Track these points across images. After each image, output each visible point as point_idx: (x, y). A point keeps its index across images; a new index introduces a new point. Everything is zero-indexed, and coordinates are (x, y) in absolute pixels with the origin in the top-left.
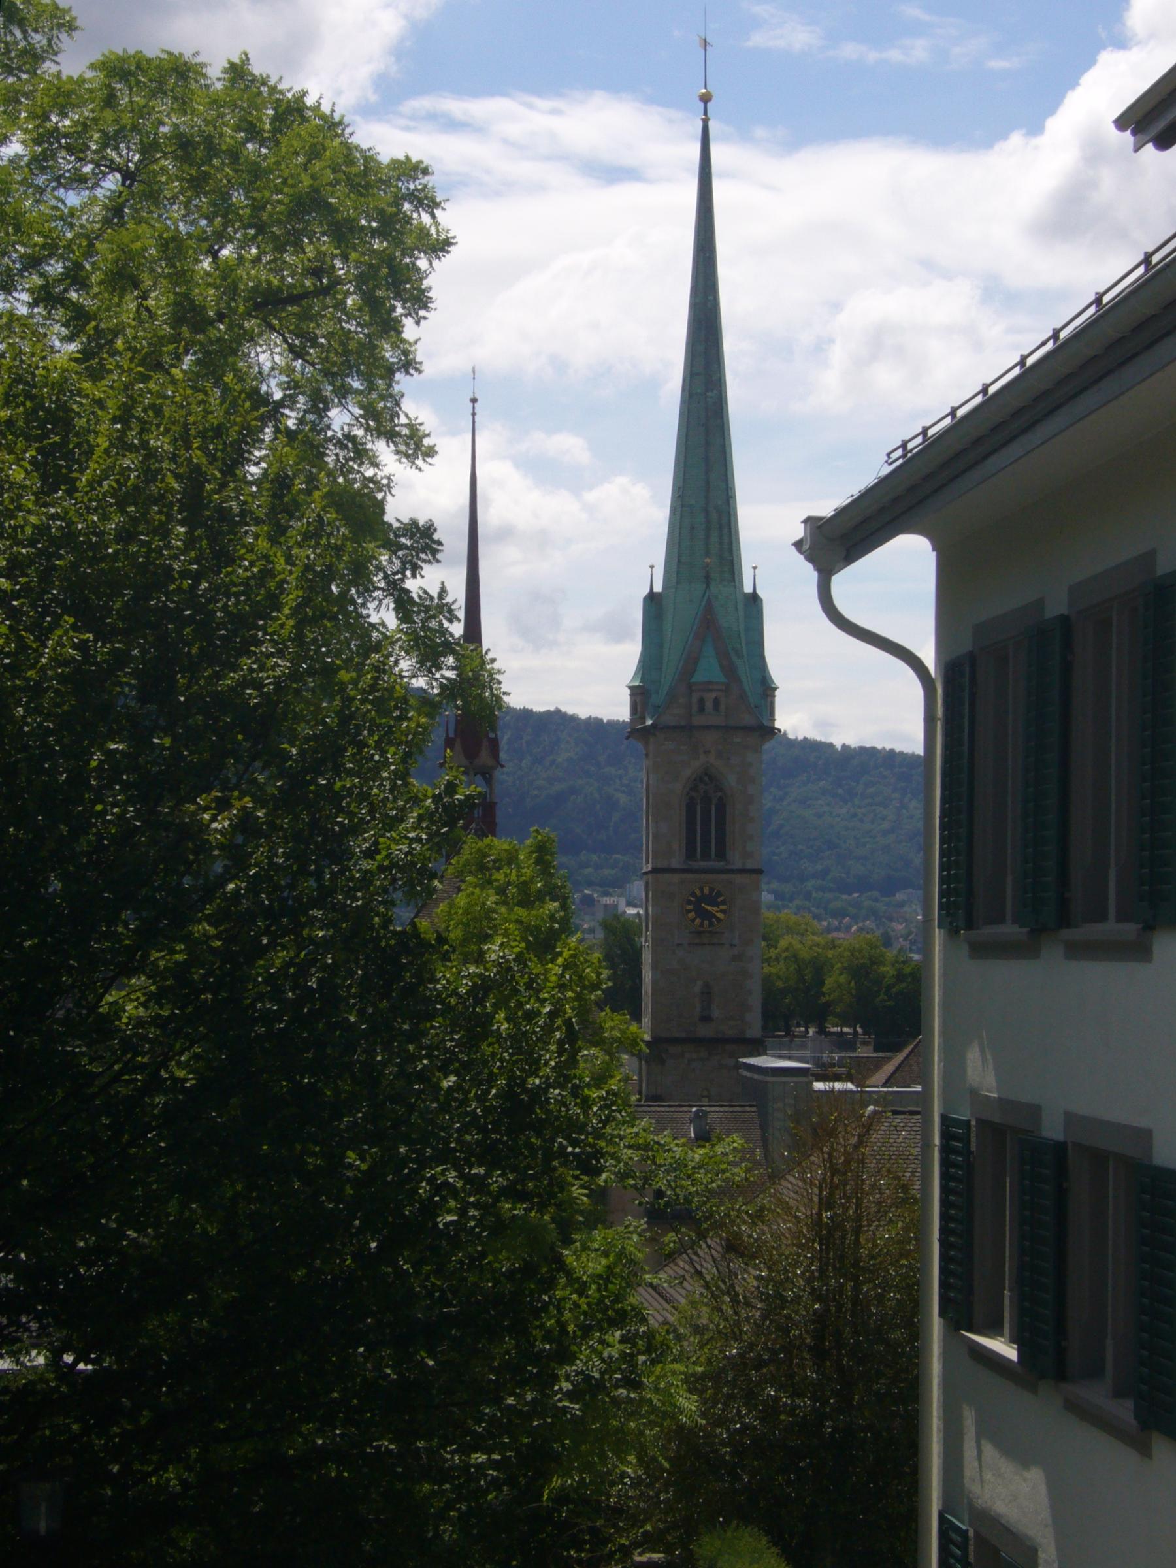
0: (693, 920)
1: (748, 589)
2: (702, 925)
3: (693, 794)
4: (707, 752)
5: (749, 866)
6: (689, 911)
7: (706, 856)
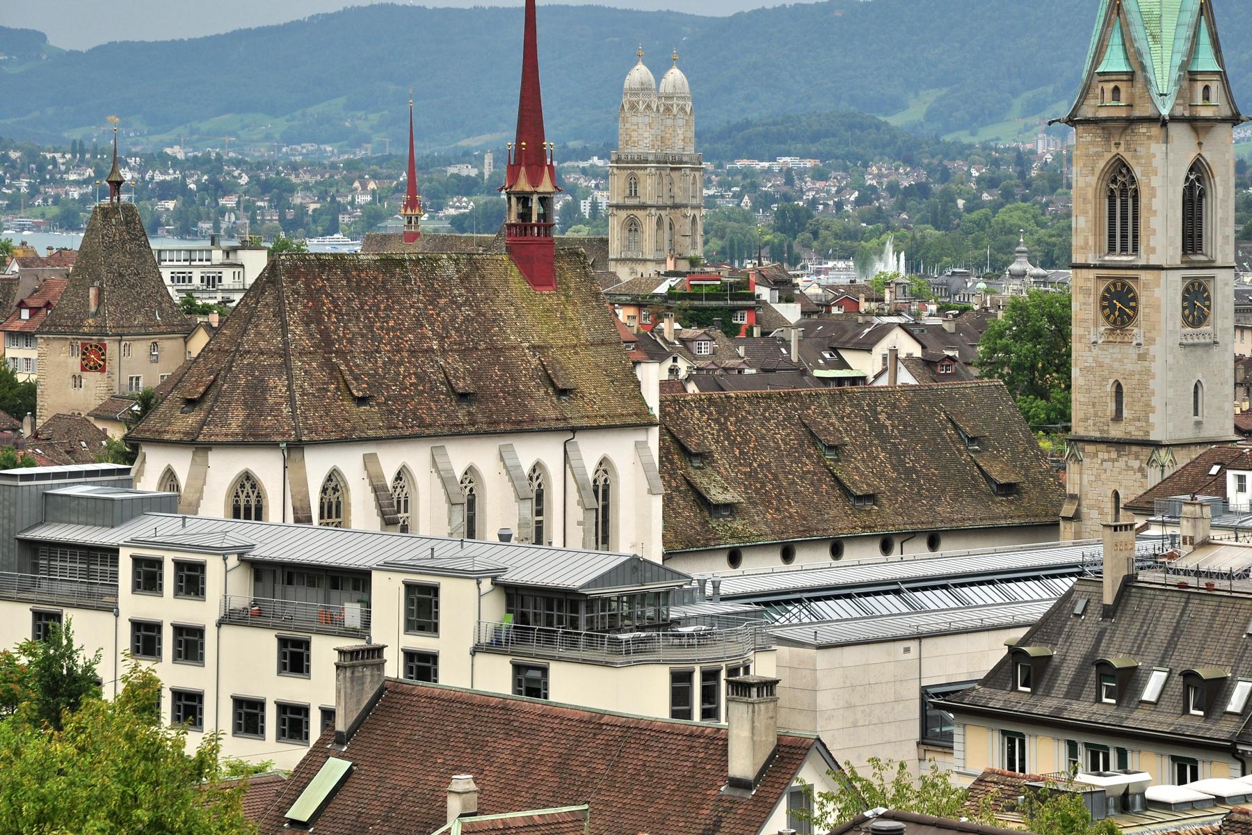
3: (1113, 186)
4: (1118, 144)
5: (1152, 263)
7: (1124, 249)
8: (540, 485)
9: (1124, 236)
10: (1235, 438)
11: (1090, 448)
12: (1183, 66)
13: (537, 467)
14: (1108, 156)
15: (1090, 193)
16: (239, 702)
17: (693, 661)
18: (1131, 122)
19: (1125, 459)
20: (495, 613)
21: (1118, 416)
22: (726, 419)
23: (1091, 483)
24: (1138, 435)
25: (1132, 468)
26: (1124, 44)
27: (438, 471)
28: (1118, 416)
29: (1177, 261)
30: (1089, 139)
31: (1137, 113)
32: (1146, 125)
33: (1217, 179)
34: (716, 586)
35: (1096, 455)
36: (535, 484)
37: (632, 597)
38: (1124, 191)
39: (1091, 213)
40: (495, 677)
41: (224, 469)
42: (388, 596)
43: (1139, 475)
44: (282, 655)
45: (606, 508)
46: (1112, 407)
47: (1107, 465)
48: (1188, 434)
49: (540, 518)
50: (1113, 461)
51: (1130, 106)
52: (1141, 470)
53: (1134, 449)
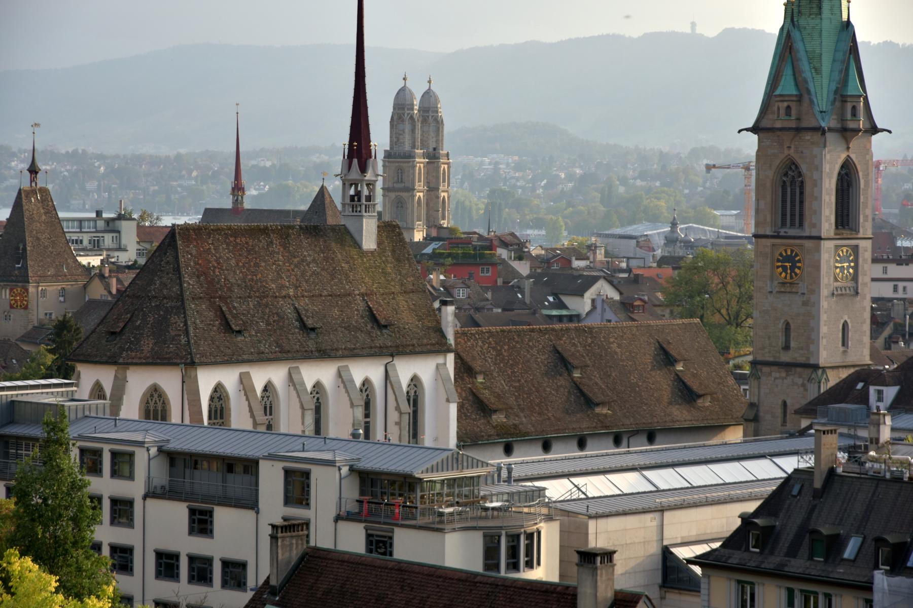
0: (781, 274)
1: (845, 17)
2: (786, 278)
4: (789, 147)
6: (778, 267)
7: (792, 225)
8: (367, 396)
9: (793, 215)
10: (870, 362)
11: (766, 369)
12: (836, 92)
13: (366, 383)
14: (782, 156)
15: (769, 184)
16: (160, 555)
17: (501, 528)
18: (798, 130)
20: (352, 492)
21: (787, 347)
22: (502, 347)
24: (801, 360)
26: (794, 75)
27: (294, 385)
28: (787, 347)
29: (832, 234)
30: (768, 143)
31: (805, 124)
32: (810, 133)
33: (861, 174)
34: (510, 471)
35: (770, 374)
36: (365, 395)
37: (452, 482)
38: (793, 182)
39: (769, 198)
40: (352, 540)
41: (139, 382)
42: (271, 481)
43: (802, 389)
44: (192, 521)
45: (415, 413)
46: (781, 341)
48: (837, 360)
49: (367, 420)
50: (783, 378)
51: (798, 119)
52: (803, 385)
53: (799, 370)
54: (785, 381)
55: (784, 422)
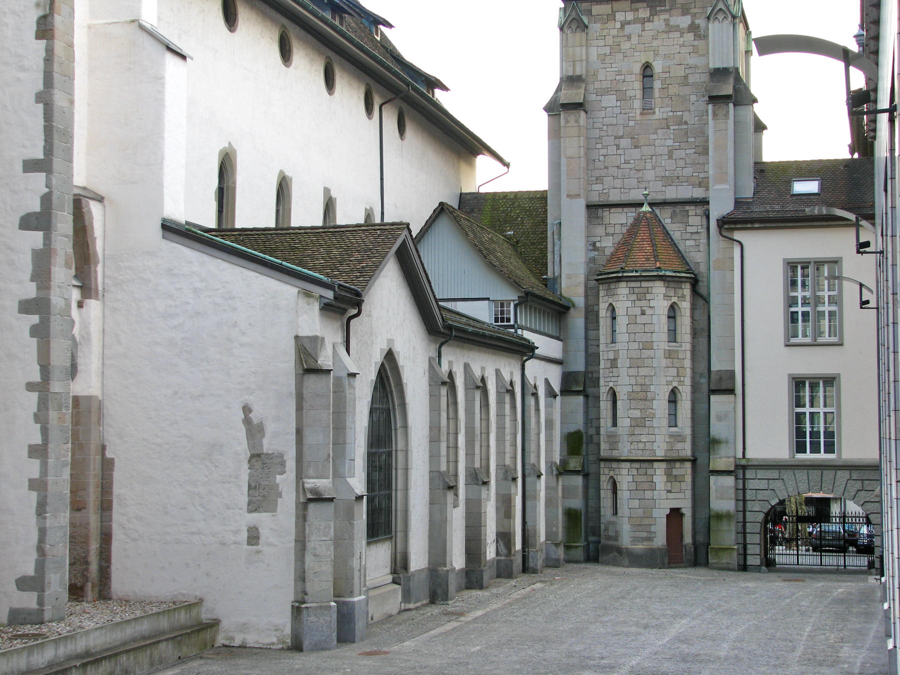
19: (663, 16)
23: (602, 58)
25: (677, 28)
35: (612, 17)
43: (690, 36)
47: (635, 29)
50: (643, 21)
52: (693, 28)
54: (648, 26)
55: (647, 110)
